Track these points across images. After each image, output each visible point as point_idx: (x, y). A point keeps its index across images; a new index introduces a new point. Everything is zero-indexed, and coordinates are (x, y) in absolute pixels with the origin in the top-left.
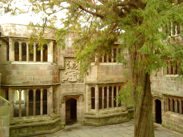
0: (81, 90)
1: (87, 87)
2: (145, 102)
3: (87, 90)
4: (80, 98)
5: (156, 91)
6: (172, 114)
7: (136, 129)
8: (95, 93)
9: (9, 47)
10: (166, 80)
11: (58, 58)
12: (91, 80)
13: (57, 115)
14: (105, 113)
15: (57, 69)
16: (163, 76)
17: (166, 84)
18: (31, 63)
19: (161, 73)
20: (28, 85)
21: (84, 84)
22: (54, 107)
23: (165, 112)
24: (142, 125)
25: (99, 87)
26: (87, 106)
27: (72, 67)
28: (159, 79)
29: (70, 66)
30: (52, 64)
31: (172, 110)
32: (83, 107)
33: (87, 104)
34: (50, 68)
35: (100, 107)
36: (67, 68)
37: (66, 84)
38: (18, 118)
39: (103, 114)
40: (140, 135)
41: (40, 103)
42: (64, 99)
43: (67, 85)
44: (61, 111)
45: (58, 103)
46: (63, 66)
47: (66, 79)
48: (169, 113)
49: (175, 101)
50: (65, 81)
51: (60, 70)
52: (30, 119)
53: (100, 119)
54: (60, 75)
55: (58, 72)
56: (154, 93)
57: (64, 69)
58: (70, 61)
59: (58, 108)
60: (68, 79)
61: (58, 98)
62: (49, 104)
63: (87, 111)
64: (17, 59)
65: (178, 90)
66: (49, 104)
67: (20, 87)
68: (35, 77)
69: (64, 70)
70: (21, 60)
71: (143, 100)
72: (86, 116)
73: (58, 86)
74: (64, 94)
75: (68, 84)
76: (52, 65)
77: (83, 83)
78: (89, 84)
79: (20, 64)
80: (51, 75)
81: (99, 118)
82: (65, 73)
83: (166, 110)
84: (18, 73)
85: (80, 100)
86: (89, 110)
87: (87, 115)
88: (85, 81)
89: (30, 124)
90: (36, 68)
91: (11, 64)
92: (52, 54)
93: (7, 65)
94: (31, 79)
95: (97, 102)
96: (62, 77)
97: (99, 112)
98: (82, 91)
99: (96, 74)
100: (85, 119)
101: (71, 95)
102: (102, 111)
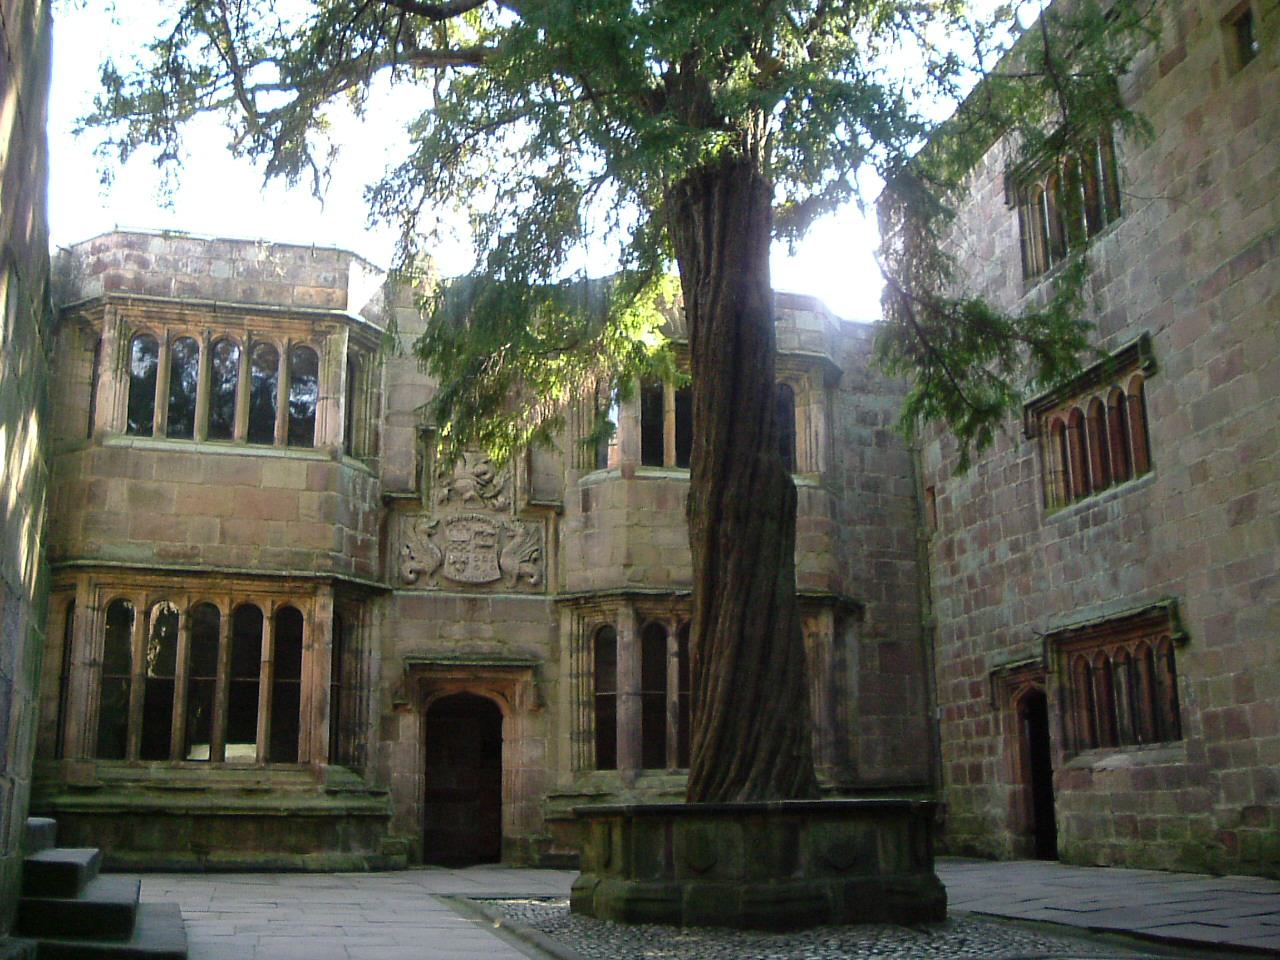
0: (529, 638)
1: (568, 624)
2: (729, 494)
3: (564, 642)
6: (1107, 755)
10: (1057, 540)
12: (589, 574)
16: (1044, 516)
17: (1061, 564)
19: (1034, 505)
20: (187, 568)
21: (543, 601)
23: (1067, 758)
25: (639, 617)
26: (566, 748)
27: (467, 495)
28: (1024, 550)
29: (459, 484)
32: (537, 753)
33: (565, 736)
34: (325, 480)
35: (652, 755)
36: (436, 500)
37: (428, 589)
38: (120, 763)
43: (435, 600)
44: (390, 763)
45: (374, 706)
46: (412, 484)
47: (427, 564)
48: (1087, 758)
49: (1117, 665)
50: (419, 573)
57: (420, 499)
59: (371, 738)
60: (441, 565)
63: (564, 780)
65: (1115, 580)
66: (310, 698)
67: (140, 579)
70: (160, 429)
73: (379, 601)
75: (442, 594)
78: (580, 602)
83: (1071, 742)
86: (578, 772)
88: (551, 587)
94: (209, 539)
95: (626, 711)
96: (405, 551)
97: (643, 783)
100: (551, 827)
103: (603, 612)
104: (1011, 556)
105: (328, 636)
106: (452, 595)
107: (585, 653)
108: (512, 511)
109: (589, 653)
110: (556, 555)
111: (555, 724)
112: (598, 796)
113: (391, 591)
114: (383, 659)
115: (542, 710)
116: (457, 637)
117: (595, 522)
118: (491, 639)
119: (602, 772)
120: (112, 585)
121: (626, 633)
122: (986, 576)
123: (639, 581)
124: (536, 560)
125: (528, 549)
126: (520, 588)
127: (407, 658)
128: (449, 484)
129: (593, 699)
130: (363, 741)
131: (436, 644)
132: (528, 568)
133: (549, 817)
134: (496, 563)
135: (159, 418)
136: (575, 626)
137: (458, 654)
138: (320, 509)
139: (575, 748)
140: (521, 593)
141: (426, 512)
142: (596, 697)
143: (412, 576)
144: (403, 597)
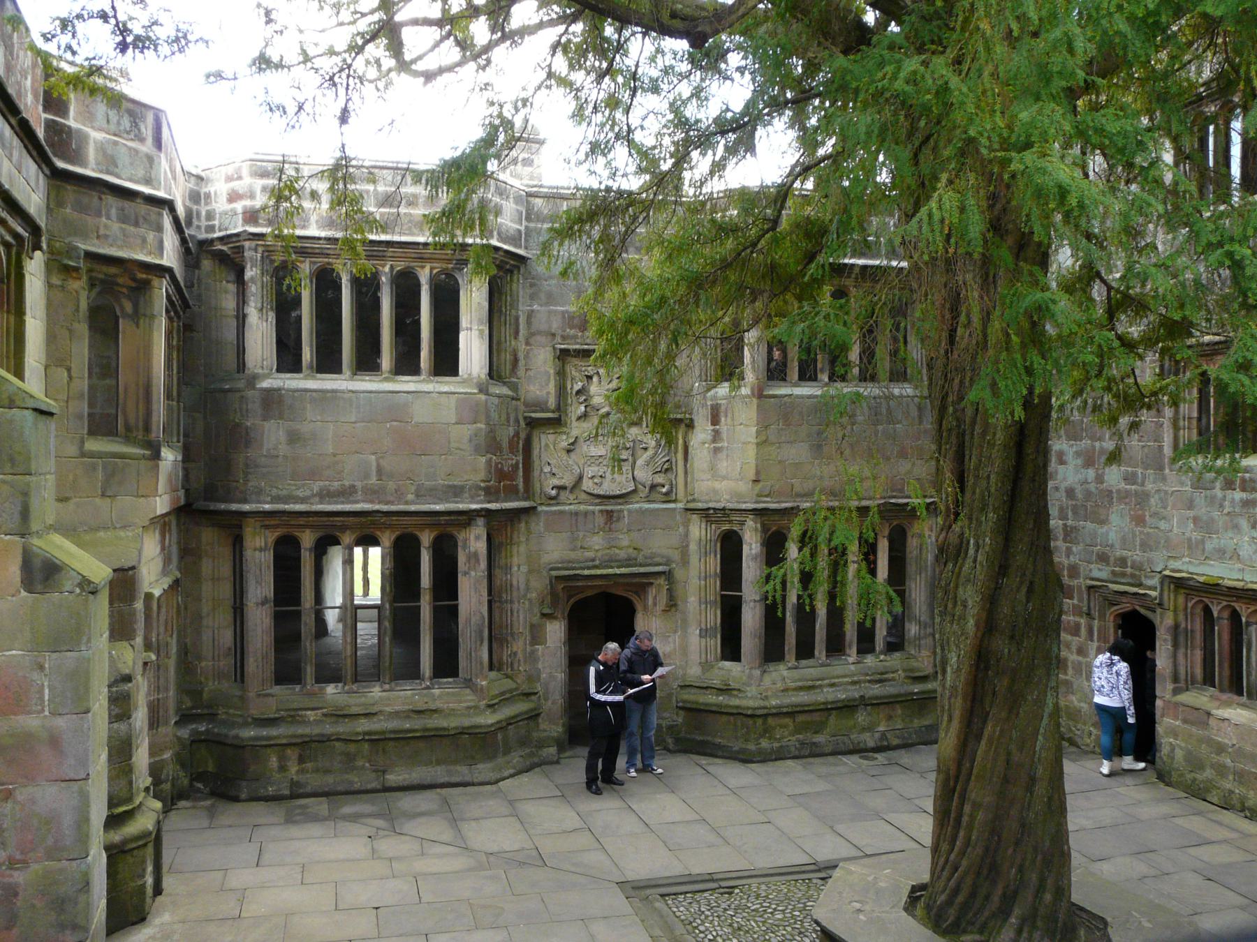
0: (660, 544)
1: (697, 530)
2: (1005, 609)
3: (693, 547)
4: (652, 592)
5: (1123, 561)
6: (1228, 704)
7: (947, 780)
8: (744, 565)
9: (248, 293)
10: (1188, 488)
11: (521, 355)
12: (717, 485)
13: (514, 686)
14: (801, 688)
15: (517, 421)
17: (1191, 513)
18: (367, 384)
19: (1161, 448)
21: (674, 509)
22: (496, 635)
23: (1176, 692)
24: (978, 759)
25: (765, 529)
28: (1143, 484)
30: (483, 389)
31: (1226, 683)
33: (694, 633)
34: (469, 411)
35: (772, 652)
36: (574, 418)
37: (569, 505)
39: (790, 693)
40: (965, 819)
41: (416, 612)
42: (553, 593)
43: (576, 514)
45: (521, 615)
46: (552, 403)
47: (567, 480)
48: (1200, 698)
50: (561, 488)
51: (533, 424)
52: (363, 699)
53: (770, 721)
54: (535, 452)
55: (523, 435)
56: (1113, 573)
58: (591, 371)
59: (519, 646)
60: (581, 478)
61: (522, 587)
62: (468, 621)
63: (694, 672)
64: (288, 358)
66: (468, 621)
67: (302, 521)
68: (383, 463)
69: (556, 423)
70: (311, 367)
71: (991, 601)
72: (686, 697)
73: (524, 517)
74: (558, 569)
75: (582, 507)
76: (483, 397)
77: (672, 505)
78: (708, 515)
79: (306, 390)
80: (477, 450)
81: (765, 711)
82: (564, 444)
83: (1182, 676)
84: (294, 438)
85: (655, 604)
86: (706, 666)
87: (693, 691)
89: (364, 725)
90: (394, 410)
91: (254, 388)
92: (481, 332)
93: (238, 395)
94: (367, 476)
95: (751, 618)
97: (767, 680)
98: (664, 551)
99: (751, 452)
100: (681, 712)
101: (599, 572)
102: (784, 674)
103: (730, 522)
104: (1123, 485)
105: (483, 564)
106: (591, 508)
107: (712, 555)
108: (644, 425)
109: (716, 556)
110: (685, 466)
111: (685, 622)
112: (726, 690)
113: (534, 508)
114: (530, 572)
115: (673, 609)
116: (597, 548)
117: (724, 436)
118: (629, 547)
119: (727, 664)
120: (276, 526)
121: (752, 545)
122: (1088, 494)
123: (766, 496)
124: (667, 470)
125: (661, 459)
126: (654, 496)
127: (552, 569)
128: (585, 400)
129: (719, 599)
130: (515, 649)
131: (578, 555)
132: (659, 479)
133: (680, 704)
134: (630, 476)
135: (307, 354)
136: (703, 532)
137: (597, 562)
138: (470, 441)
139: (703, 644)
140: (653, 502)
141: (565, 429)
142: (722, 596)
143: (554, 492)
144: (546, 512)
